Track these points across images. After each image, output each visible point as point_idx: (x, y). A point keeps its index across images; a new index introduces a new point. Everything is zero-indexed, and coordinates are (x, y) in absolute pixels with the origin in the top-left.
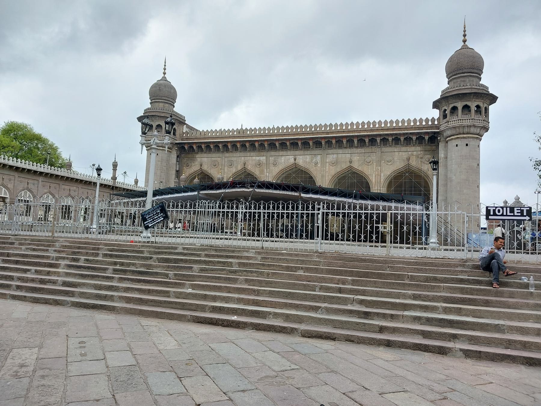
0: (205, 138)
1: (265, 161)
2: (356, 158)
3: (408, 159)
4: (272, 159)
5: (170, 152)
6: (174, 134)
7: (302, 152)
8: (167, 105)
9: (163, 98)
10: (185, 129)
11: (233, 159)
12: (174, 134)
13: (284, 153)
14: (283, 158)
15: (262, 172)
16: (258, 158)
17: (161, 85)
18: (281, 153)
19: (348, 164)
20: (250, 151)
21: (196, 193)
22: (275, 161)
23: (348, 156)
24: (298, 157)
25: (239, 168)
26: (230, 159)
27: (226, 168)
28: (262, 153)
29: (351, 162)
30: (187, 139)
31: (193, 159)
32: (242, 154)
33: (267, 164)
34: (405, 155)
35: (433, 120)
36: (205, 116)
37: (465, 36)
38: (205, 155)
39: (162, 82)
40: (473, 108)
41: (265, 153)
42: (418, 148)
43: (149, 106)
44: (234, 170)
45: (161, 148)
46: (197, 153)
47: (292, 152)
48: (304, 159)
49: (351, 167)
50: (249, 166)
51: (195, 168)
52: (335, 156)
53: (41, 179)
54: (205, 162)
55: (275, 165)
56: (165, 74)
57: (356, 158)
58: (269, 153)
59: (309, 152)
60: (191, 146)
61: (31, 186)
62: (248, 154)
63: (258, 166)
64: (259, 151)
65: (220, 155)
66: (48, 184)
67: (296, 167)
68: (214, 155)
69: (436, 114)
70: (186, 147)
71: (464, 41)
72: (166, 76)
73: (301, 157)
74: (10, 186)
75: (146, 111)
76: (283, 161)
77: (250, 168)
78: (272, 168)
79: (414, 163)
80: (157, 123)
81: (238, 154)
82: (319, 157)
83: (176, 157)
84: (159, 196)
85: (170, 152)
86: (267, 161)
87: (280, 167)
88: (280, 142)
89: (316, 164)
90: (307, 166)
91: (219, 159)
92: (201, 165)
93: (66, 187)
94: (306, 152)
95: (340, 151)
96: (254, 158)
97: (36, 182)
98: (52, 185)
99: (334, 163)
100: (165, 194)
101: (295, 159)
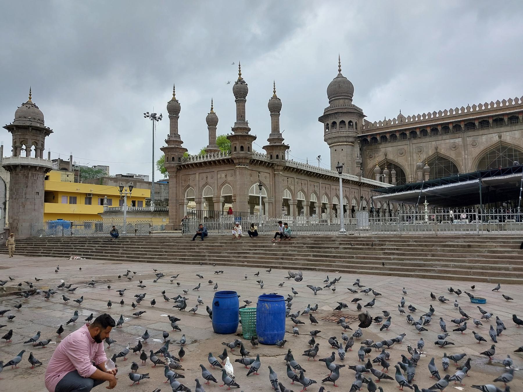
0: (388, 128)
1: (461, 143)
4: (469, 140)
5: (353, 146)
6: (356, 129)
7: (508, 128)
8: (347, 101)
9: (343, 94)
11: (421, 145)
12: (356, 129)
13: (486, 131)
14: (484, 137)
15: (459, 154)
16: (452, 141)
17: (340, 82)
18: (481, 132)
20: (441, 135)
21: (477, 181)
22: (474, 141)
24: (503, 135)
25: (431, 153)
26: (419, 145)
27: (415, 155)
28: (457, 135)
30: (368, 131)
31: (377, 150)
32: (433, 138)
33: (465, 146)
36: (378, 106)
38: (390, 144)
39: (339, 79)
41: (460, 135)
43: (329, 105)
44: (424, 156)
45: (345, 143)
46: (381, 144)
47: (496, 130)
50: (443, 150)
51: (379, 158)
53: (321, 181)
54: (389, 151)
56: (340, 71)
58: (465, 134)
59: (517, 127)
60: (374, 138)
61: (316, 189)
63: (454, 149)
64: (453, 133)
65: (407, 142)
66: (324, 185)
67: (501, 145)
68: (400, 143)
70: (369, 139)
72: (341, 72)
73: (508, 134)
74: (306, 190)
75: (326, 110)
76: (484, 140)
77: (443, 151)
78: (471, 149)
80: (340, 120)
81: (427, 139)
83: (359, 150)
84: (430, 187)
85: (353, 146)
86: (464, 142)
87: (482, 148)
88: (480, 121)
90: (516, 143)
91: (406, 147)
92: (386, 155)
94: (514, 128)
96: (447, 141)
97: (318, 184)
98: (327, 186)
100: (437, 185)
101: (500, 137)
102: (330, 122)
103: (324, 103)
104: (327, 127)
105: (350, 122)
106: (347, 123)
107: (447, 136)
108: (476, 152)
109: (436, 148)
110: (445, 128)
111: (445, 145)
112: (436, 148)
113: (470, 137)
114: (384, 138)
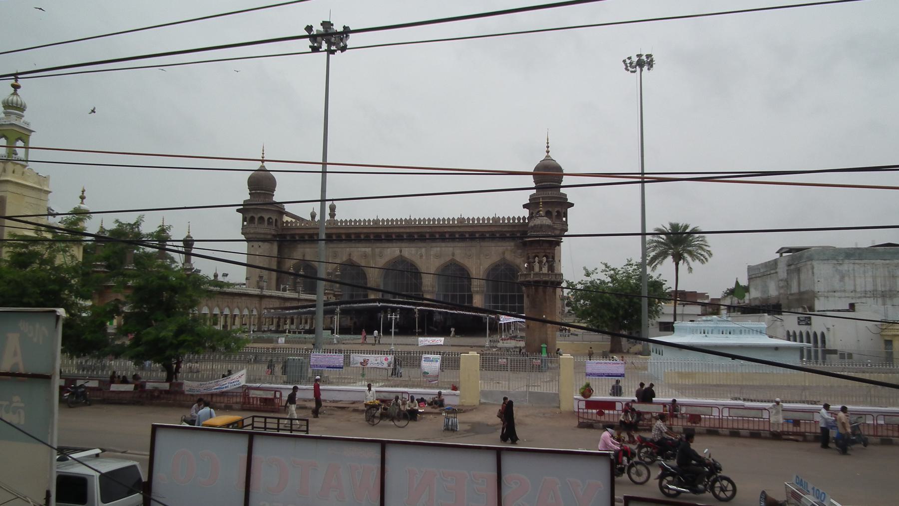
2: (458, 252)
3: (504, 253)
4: (377, 250)
10: (286, 218)
13: (390, 245)
16: (363, 249)
18: (387, 245)
19: (451, 257)
23: (451, 249)
24: (403, 250)
25: (345, 258)
28: (368, 245)
29: (453, 255)
34: (501, 249)
35: (524, 218)
37: (548, 147)
40: (555, 214)
42: (512, 244)
43: (248, 197)
47: (399, 244)
48: (410, 252)
49: (453, 260)
52: (438, 249)
55: (381, 256)
57: (458, 252)
60: (293, 236)
62: (353, 245)
69: (526, 213)
71: (548, 152)
77: (356, 258)
79: (509, 257)
80: (259, 215)
81: (343, 245)
82: (423, 250)
89: (421, 256)
93: (237, 300)
95: (443, 244)
99: (437, 256)
101: (401, 251)
102: (248, 216)
103: (244, 195)
104: (244, 220)
105: (270, 218)
106: (266, 219)
107: (360, 245)
108: (381, 262)
109: (350, 255)
110: (358, 235)
111: (358, 253)
112: (350, 255)
113: (378, 248)
114: (302, 236)
